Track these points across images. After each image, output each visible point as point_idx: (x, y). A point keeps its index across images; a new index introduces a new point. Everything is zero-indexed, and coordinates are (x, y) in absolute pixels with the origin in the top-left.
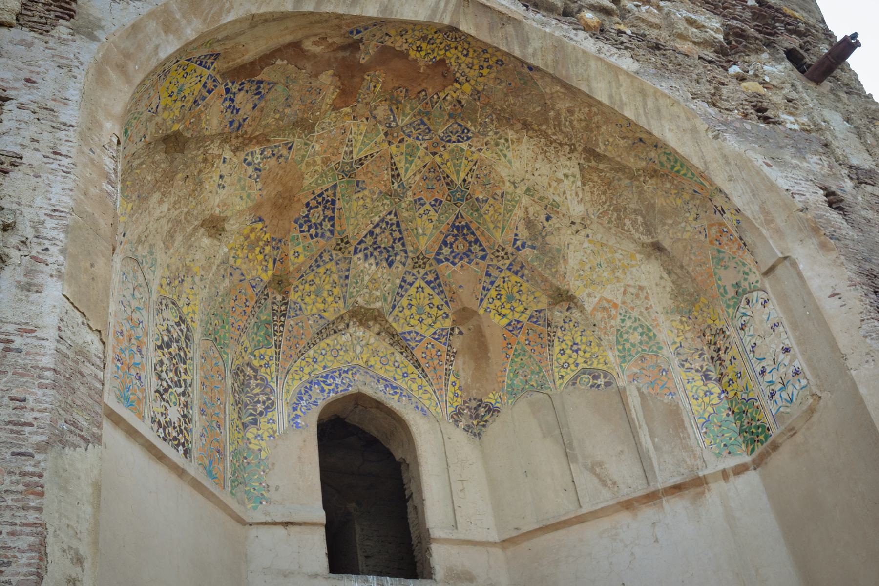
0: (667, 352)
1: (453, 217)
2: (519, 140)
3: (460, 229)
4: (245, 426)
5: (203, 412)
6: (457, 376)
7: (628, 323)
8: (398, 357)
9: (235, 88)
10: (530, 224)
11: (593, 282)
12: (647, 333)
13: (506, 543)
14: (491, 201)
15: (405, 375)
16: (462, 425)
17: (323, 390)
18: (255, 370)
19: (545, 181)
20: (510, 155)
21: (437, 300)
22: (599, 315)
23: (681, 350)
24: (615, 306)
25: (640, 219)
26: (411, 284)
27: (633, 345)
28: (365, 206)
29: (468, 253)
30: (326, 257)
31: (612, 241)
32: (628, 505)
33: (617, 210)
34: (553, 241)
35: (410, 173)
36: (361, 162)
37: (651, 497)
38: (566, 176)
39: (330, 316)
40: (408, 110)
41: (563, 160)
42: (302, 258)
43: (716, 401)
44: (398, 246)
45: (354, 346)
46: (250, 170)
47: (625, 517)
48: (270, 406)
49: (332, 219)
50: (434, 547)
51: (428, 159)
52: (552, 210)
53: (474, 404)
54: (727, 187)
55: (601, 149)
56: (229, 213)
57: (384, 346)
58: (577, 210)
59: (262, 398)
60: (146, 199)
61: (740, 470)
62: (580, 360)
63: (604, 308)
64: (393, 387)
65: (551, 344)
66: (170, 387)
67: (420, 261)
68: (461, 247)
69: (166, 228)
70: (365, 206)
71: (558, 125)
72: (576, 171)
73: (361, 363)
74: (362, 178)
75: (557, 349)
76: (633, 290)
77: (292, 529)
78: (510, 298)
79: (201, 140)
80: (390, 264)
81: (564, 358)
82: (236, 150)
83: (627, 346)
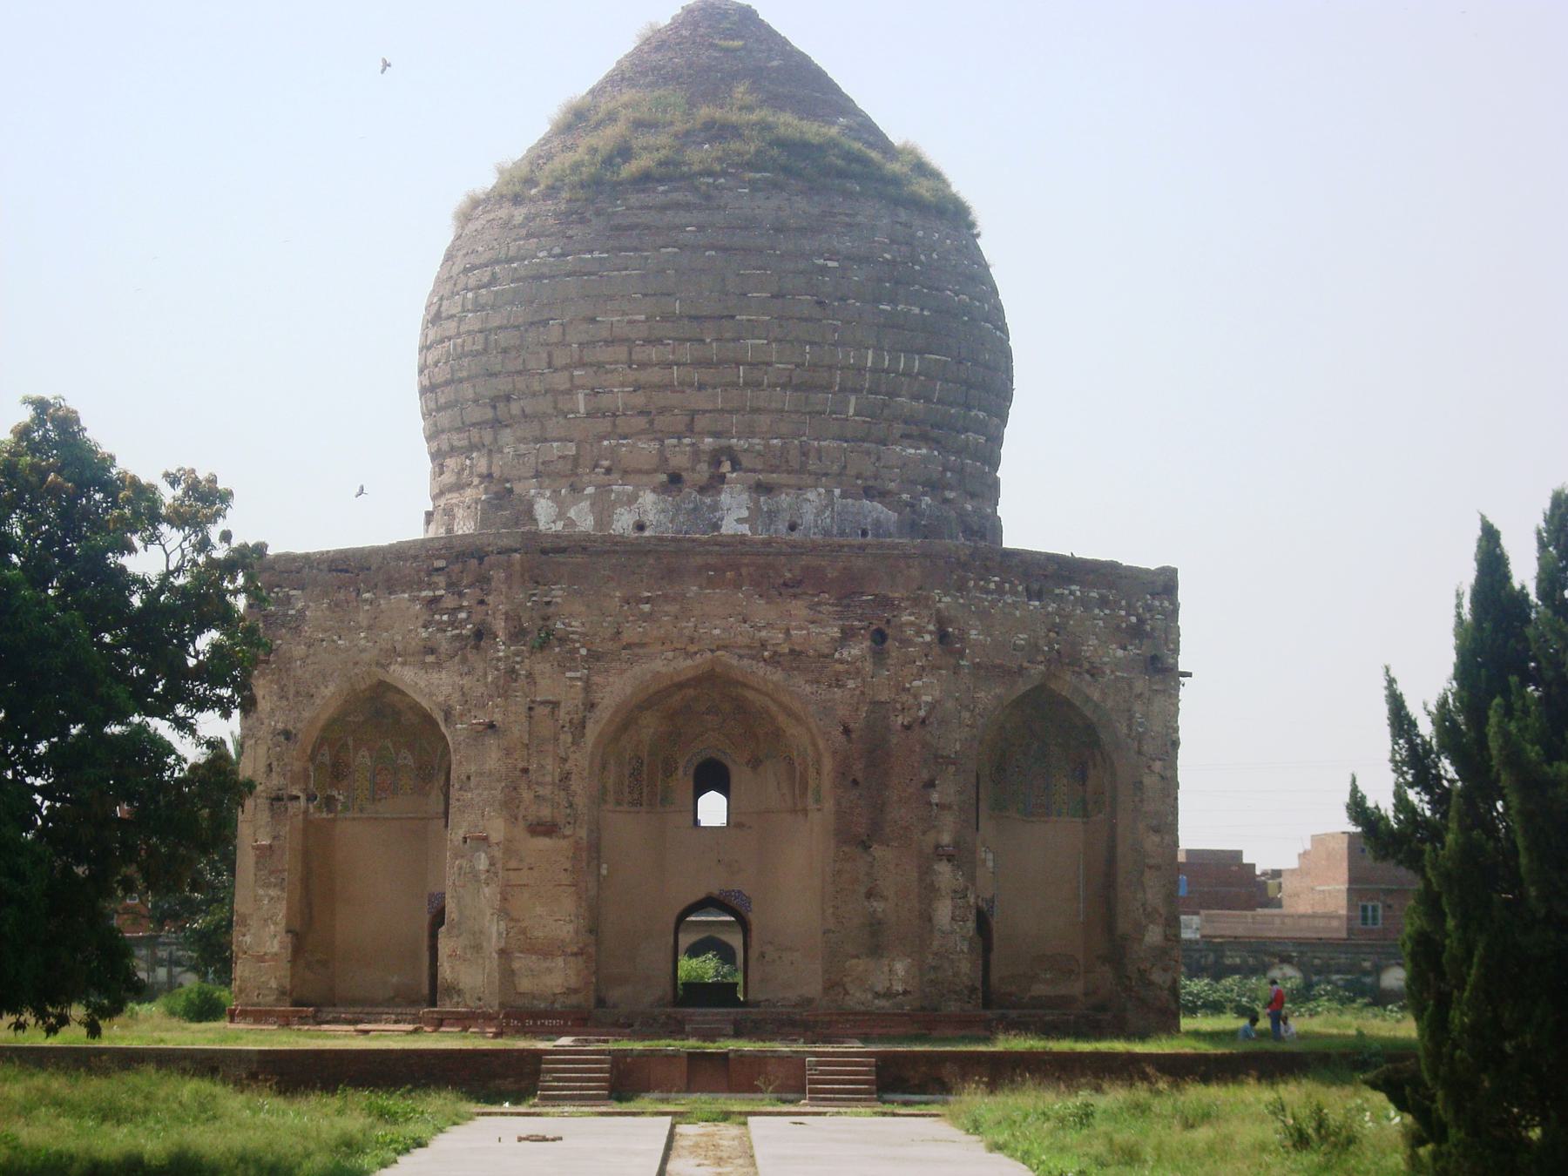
0: (809, 759)
4: (667, 777)
48: (676, 769)
61: (819, 810)
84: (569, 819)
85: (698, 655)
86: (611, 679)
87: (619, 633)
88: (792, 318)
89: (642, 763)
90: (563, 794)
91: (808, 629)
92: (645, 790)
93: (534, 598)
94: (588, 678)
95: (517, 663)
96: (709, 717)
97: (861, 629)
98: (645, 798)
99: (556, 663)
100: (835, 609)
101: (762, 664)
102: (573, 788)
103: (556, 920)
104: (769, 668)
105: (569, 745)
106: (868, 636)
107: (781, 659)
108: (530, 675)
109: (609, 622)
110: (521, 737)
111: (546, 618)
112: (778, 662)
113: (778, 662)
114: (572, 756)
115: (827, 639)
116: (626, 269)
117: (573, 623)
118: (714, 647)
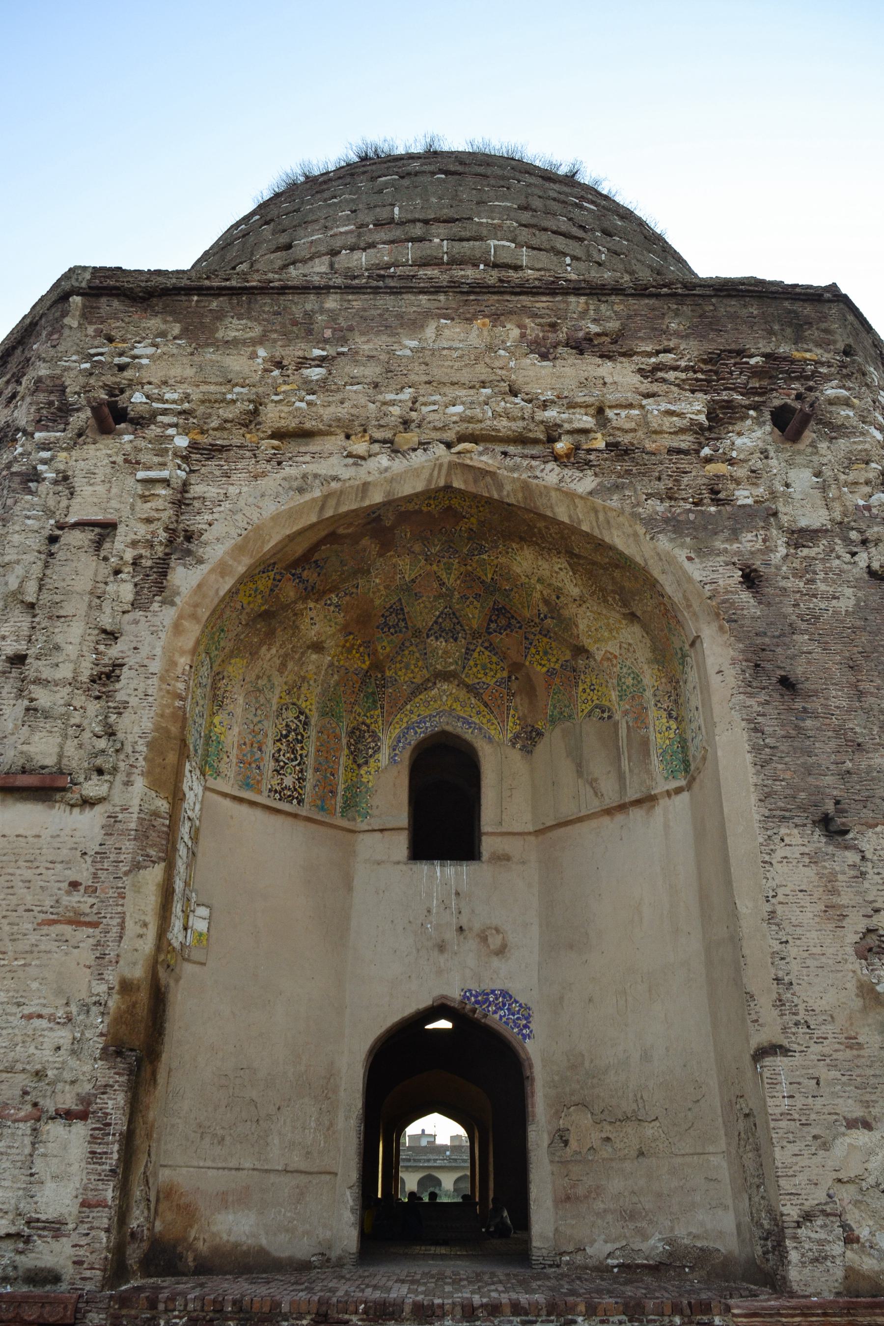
0: (649, 694)
1: (492, 604)
2: (522, 548)
3: (499, 611)
4: (359, 766)
5: (316, 770)
6: (516, 709)
7: (625, 670)
8: (473, 700)
9: (299, 571)
10: (546, 602)
11: (599, 640)
12: (637, 678)
13: (537, 833)
14: (515, 590)
15: (478, 713)
16: (518, 746)
17: (416, 733)
18: (368, 726)
19: (548, 573)
20: (518, 558)
21: (494, 659)
22: (606, 664)
23: (657, 693)
24: (616, 657)
25: (617, 597)
26: (474, 650)
27: (628, 687)
28: (425, 607)
29: (509, 626)
30: (407, 644)
31: (604, 612)
32: (609, 812)
33: (601, 590)
34: (566, 613)
35: (451, 580)
36: (413, 581)
37: (622, 808)
38: (561, 569)
39: (418, 680)
40: (436, 542)
41: (555, 559)
42: (388, 649)
43: (672, 736)
44: (458, 627)
45: (441, 696)
46: (332, 608)
47: (606, 820)
48: (377, 750)
49: (404, 620)
50: (484, 838)
51: (463, 569)
52: (559, 592)
53: (529, 729)
54: (661, 578)
55: (576, 551)
56: (323, 638)
57: (462, 694)
58: (575, 591)
59: (373, 745)
60: (256, 653)
61: (678, 791)
62: (595, 698)
63: (608, 659)
64: (469, 723)
65: (577, 685)
66: (286, 764)
67: (476, 635)
68: (503, 622)
69: (278, 662)
70: (425, 607)
71: (543, 537)
72: (566, 565)
73: (446, 708)
74: (418, 590)
75: (581, 689)
76: (624, 645)
77: (386, 833)
78: (546, 653)
79: (285, 607)
80: (456, 640)
81: (585, 696)
82: (317, 601)
83: (624, 687)
84: (99, 761)
85: (420, 452)
86: (233, 490)
87: (256, 412)
88: (545, 230)
89: (306, 724)
90: (93, 707)
91: (642, 407)
92: (309, 774)
93: (96, 358)
94: (186, 485)
95: (44, 462)
96: (442, 644)
97: (749, 407)
98: (308, 785)
99: (120, 459)
100: (691, 374)
101: (551, 465)
102: (120, 696)
103: (29, 1017)
104: (568, 472)
105: (127, 607)
106: (767, 416)
107: (592, 457)
108: (64, 478)
109: (238, 394)
110: (20, 590)
111: (115, 391)
112: (588, 463)
113: (588, 463)
114: (126, 628)
115: (685, 422)
116: (335, 197)
117: (167, 396)
118: (450, 436)
